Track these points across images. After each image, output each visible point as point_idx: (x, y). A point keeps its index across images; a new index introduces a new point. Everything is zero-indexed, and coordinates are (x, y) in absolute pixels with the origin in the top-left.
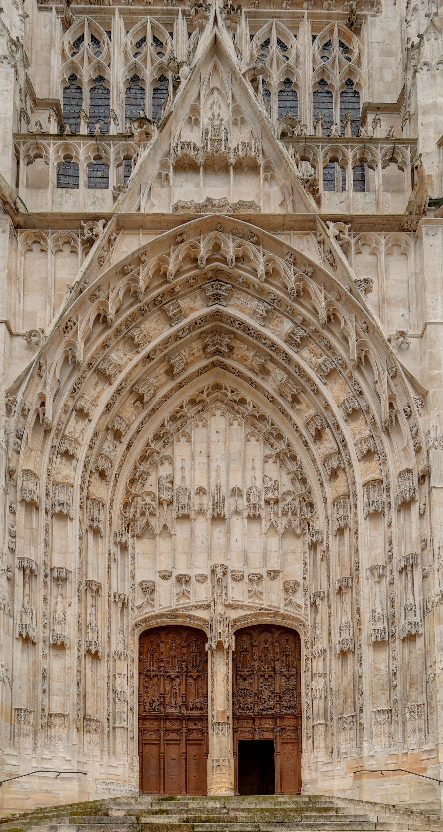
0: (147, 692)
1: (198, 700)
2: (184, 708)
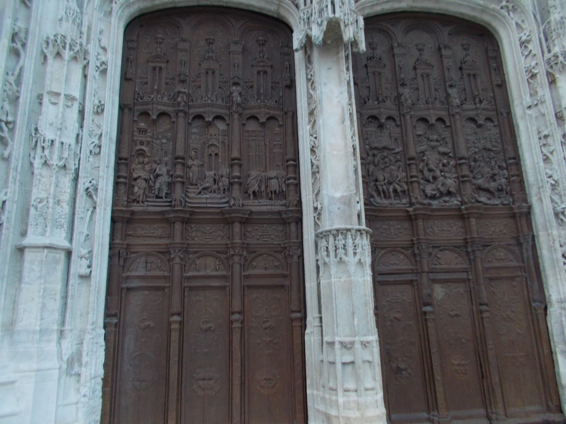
0: (141, 153)
1: (272, 173)
2: (236, 192)
